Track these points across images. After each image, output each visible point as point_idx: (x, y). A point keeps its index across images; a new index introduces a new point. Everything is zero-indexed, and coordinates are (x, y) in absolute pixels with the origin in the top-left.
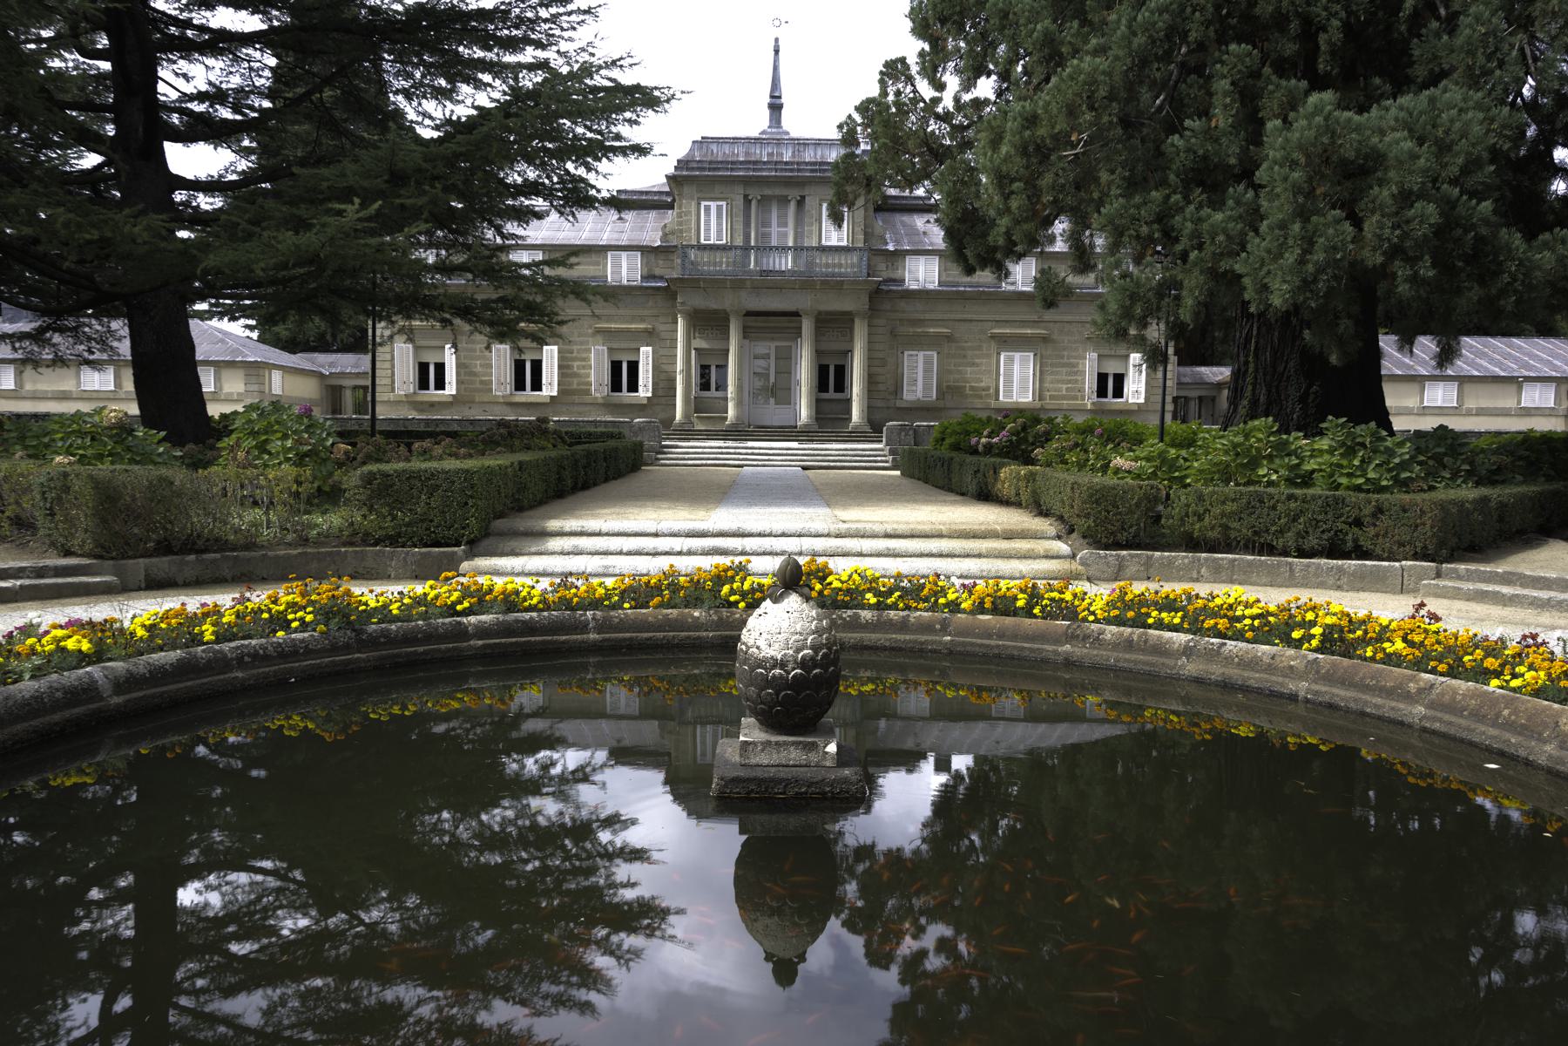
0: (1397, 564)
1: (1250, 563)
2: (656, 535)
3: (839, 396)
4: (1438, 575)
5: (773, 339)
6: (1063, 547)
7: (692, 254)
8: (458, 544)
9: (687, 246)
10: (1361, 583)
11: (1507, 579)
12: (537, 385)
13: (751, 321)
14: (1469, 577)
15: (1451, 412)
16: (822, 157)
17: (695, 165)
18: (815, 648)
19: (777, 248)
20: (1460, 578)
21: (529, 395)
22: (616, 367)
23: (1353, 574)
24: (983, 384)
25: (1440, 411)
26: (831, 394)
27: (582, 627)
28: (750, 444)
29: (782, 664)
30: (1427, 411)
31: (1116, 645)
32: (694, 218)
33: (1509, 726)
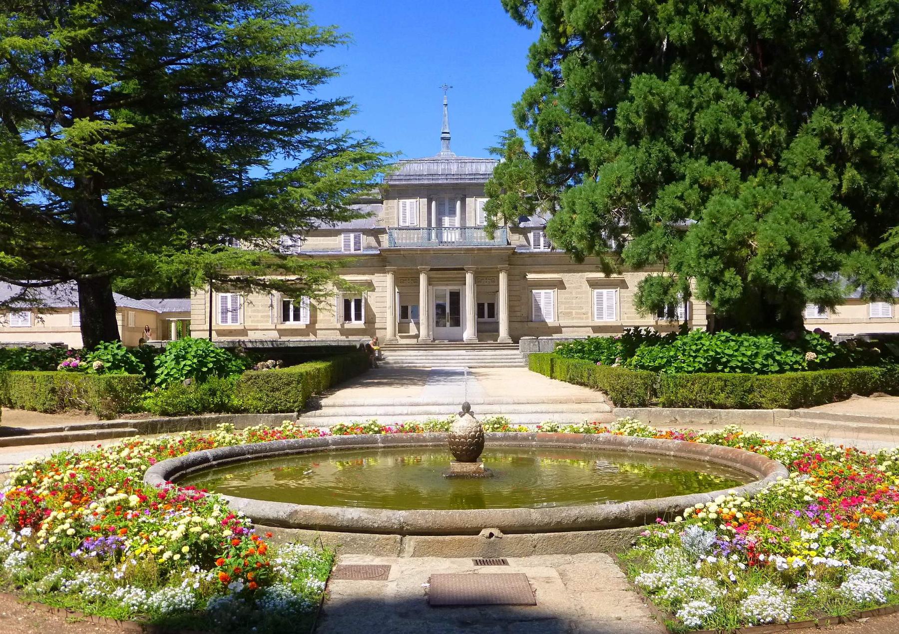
0: (770, 411)
1: (700, 413)
2: (393, 405)
3: (491, 320)
4: (791, 415)
5: (447, 285)
6: (607, 407)
7: (395, 233)
8: (293, 411)
9: (392, 229)
10: (755, 421)
11: (821, 416)
12: (297, 317)
13: (434, 274)
14: (806, 416)
15: (888, 320)
16: (477, 169)
17: (396, 178)
18: (476, 432)
19: (449, 228)
20: (801, 417)
21: (291, 324)
22: (347, 304)
23: (750, 416)
24: (583, 311)
25: (880, 321)
26: (486, 318)
27: (375, 441)
28: (435, 352)
29: (465, 438)
30: (872, 321)
31: (604, 443)
32: (396, 210)
33: (731, 460)
